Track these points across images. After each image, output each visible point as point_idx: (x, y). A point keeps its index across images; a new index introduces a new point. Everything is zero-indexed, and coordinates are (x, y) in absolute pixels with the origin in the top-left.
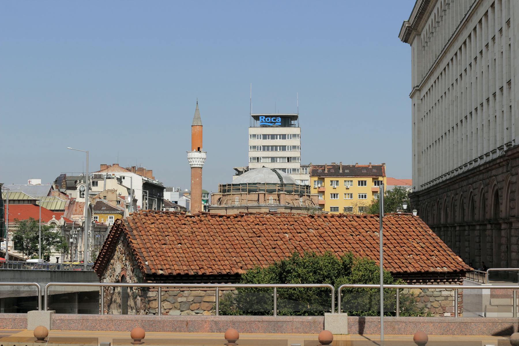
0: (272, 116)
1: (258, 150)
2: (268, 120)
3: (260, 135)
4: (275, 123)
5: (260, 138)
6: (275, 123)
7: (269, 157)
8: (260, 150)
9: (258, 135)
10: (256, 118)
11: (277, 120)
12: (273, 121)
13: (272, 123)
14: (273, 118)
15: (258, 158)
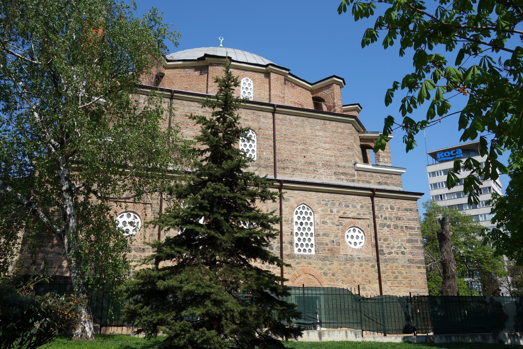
0: (449, 150)
1: (440, 187)
2: (447, 154)
3: (440, 171)
4: (455, 155)
5: (441, 174)
6: (455, 155)
7: (454, 193)
8: (443, 186)
9: (437, 172)
10: (434, 155)
11: (457, 153)
12: (452, 153)
13: (451, 156)
14: (452, 152)
15: (441, 196)
